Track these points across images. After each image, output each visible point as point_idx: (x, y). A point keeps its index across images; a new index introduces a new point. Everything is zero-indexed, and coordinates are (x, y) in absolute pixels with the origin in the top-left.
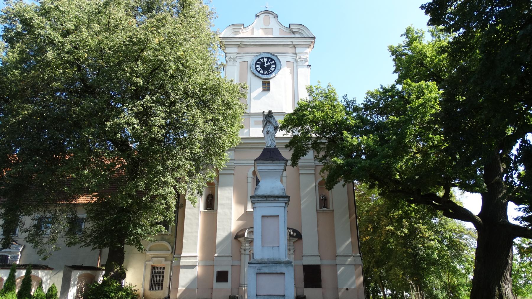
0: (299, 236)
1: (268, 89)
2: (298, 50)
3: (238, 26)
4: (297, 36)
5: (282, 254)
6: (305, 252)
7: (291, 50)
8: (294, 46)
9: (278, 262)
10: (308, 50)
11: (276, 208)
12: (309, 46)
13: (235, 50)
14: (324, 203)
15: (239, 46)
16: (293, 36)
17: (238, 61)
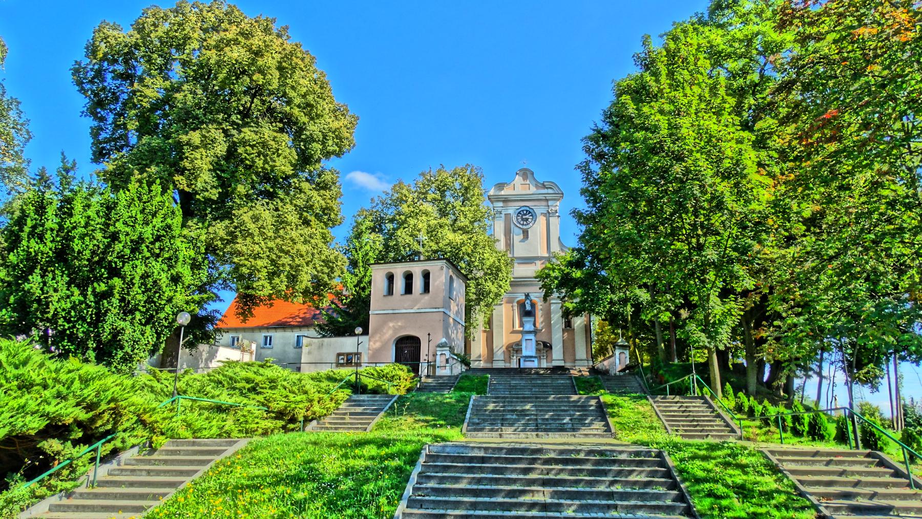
0: (551, 347)
1: (527, 237)
2: (550, 203)
3: (500, 186)
4: (550, 191)
5: (534, 354)
6: (554, 357)
7: (544, 203)
8: (547, 200)
9: (531, 357)
10: (558, 203)
11: (532, 337)
12: (558, 200)
13: (501, 204)
14: (568, 324)
15: (504, 201)
16: (545, 191)
17: (503, 213)
